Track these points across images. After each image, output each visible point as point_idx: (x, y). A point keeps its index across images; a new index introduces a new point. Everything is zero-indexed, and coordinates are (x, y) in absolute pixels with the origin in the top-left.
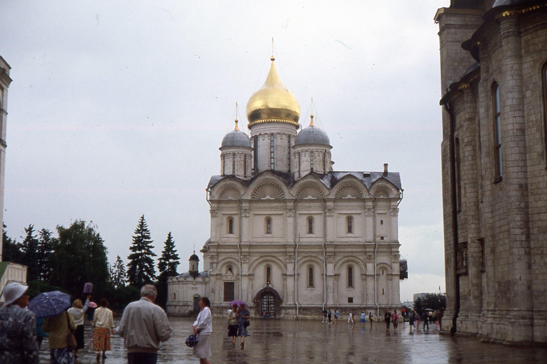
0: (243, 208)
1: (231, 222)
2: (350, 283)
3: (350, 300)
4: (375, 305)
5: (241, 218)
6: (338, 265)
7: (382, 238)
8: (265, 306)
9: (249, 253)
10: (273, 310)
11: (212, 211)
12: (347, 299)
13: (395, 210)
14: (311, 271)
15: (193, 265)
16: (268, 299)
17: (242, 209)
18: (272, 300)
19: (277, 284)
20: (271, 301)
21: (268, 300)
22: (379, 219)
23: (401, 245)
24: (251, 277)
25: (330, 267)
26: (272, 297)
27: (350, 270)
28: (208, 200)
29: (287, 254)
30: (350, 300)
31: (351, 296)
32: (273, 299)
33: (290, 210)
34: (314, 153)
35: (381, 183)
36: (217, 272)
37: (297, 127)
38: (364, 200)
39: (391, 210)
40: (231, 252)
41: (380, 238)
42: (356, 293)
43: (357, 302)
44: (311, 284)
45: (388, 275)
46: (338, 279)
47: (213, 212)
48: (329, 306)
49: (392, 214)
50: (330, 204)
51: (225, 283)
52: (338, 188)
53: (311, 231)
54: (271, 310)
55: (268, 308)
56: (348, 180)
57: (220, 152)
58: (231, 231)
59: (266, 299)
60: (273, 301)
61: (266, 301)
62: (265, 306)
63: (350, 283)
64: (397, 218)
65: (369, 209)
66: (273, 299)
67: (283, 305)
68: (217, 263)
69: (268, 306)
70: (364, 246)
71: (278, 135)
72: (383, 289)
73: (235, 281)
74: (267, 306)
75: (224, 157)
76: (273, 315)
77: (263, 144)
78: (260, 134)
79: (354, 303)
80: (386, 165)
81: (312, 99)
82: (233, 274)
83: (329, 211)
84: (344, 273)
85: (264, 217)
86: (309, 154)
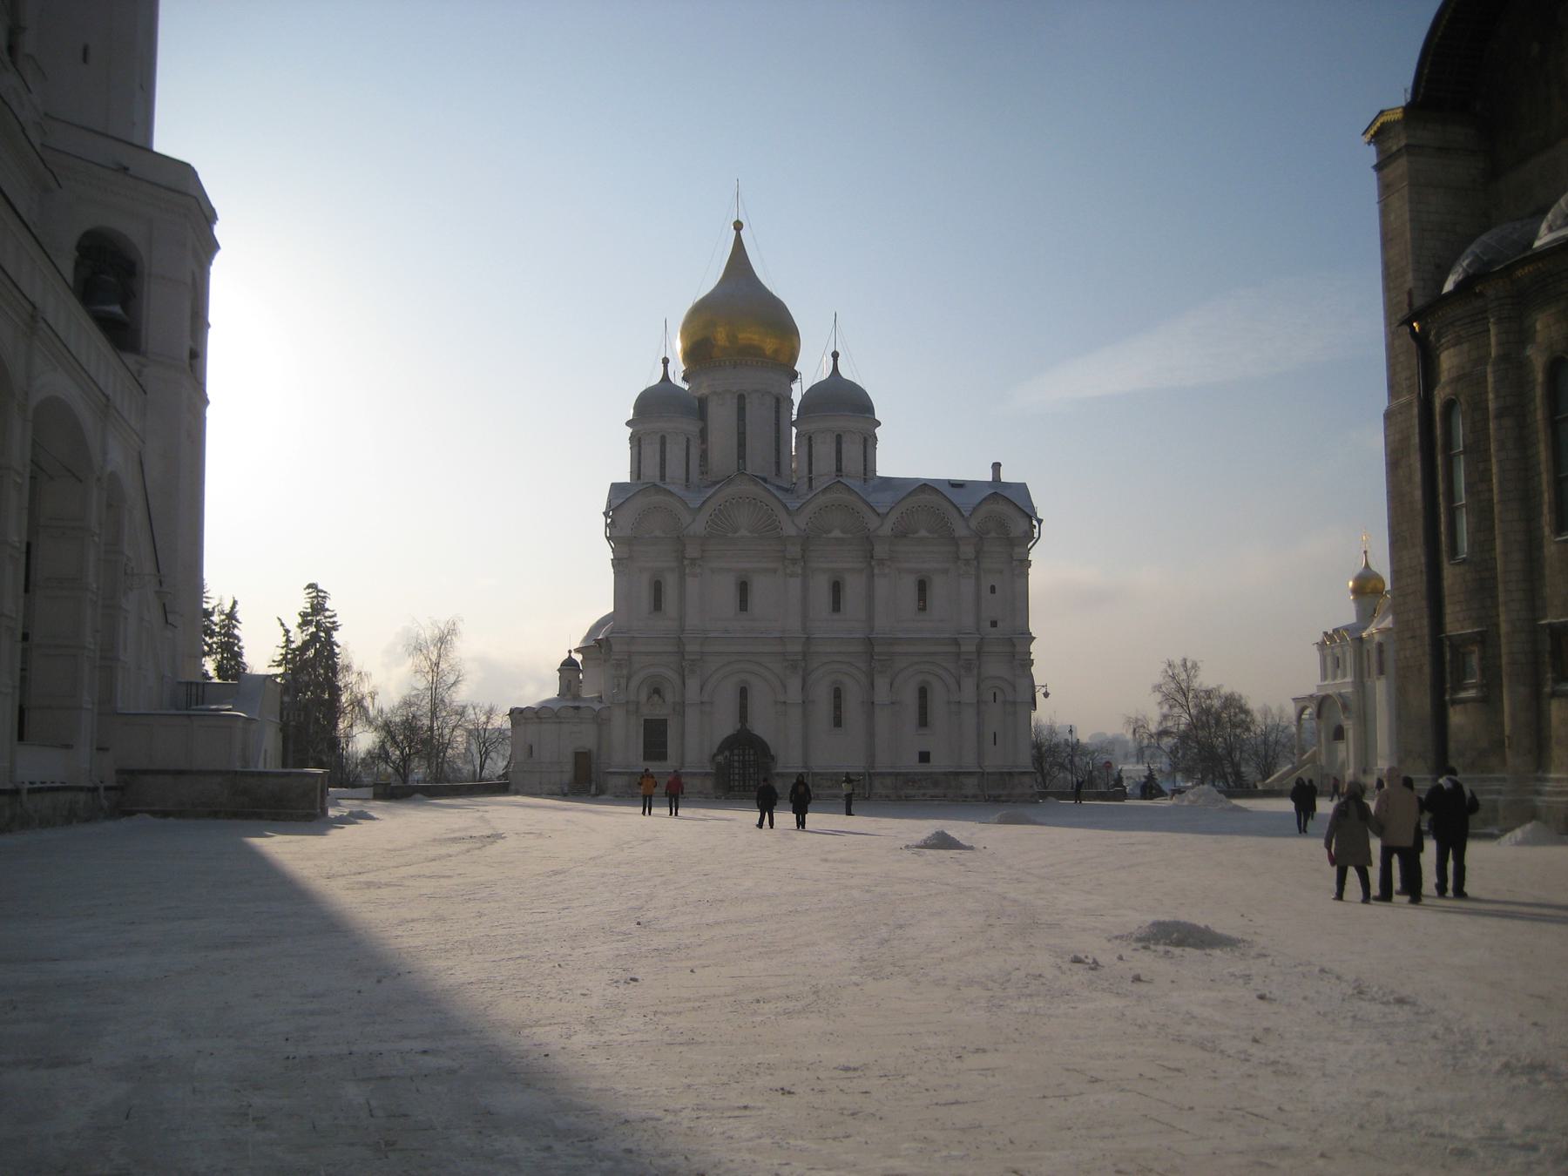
0: (687, 556)
1: (658, 588)
2: (923, 721)
3: (924, 757)
5: (682, 577)
7: (994, 624)
8: (737, 771)
11: (616, 562)
12: (917, 758)
14: (838, 694)
17: (684, 558)
19: (761, 726)
21: (744, 757)
23: (1035, 638)
25: (881, 683)
26: (752, 752)
27: (923, 693)
30: (924, 757)
31: (924, 749)
33: (794, 561)
37: (794, 376)
38: (954, 541)
39: (1014, 563)
41: (989, 623)
43: (939, 763)
44: (838, 722)
47: (617, 563)
51: (646, 721)
57: (629, 430)
58: (657, 604)
59: (739, 756)
62: (737, 771)
63: (923, 721)
67: (779, 770)
68: (629, 678)
70: (956, 642)
75: (639, 440)
77: (721, 417)
80: (996, 467)
82: (664, 701)
84: (910, 698)
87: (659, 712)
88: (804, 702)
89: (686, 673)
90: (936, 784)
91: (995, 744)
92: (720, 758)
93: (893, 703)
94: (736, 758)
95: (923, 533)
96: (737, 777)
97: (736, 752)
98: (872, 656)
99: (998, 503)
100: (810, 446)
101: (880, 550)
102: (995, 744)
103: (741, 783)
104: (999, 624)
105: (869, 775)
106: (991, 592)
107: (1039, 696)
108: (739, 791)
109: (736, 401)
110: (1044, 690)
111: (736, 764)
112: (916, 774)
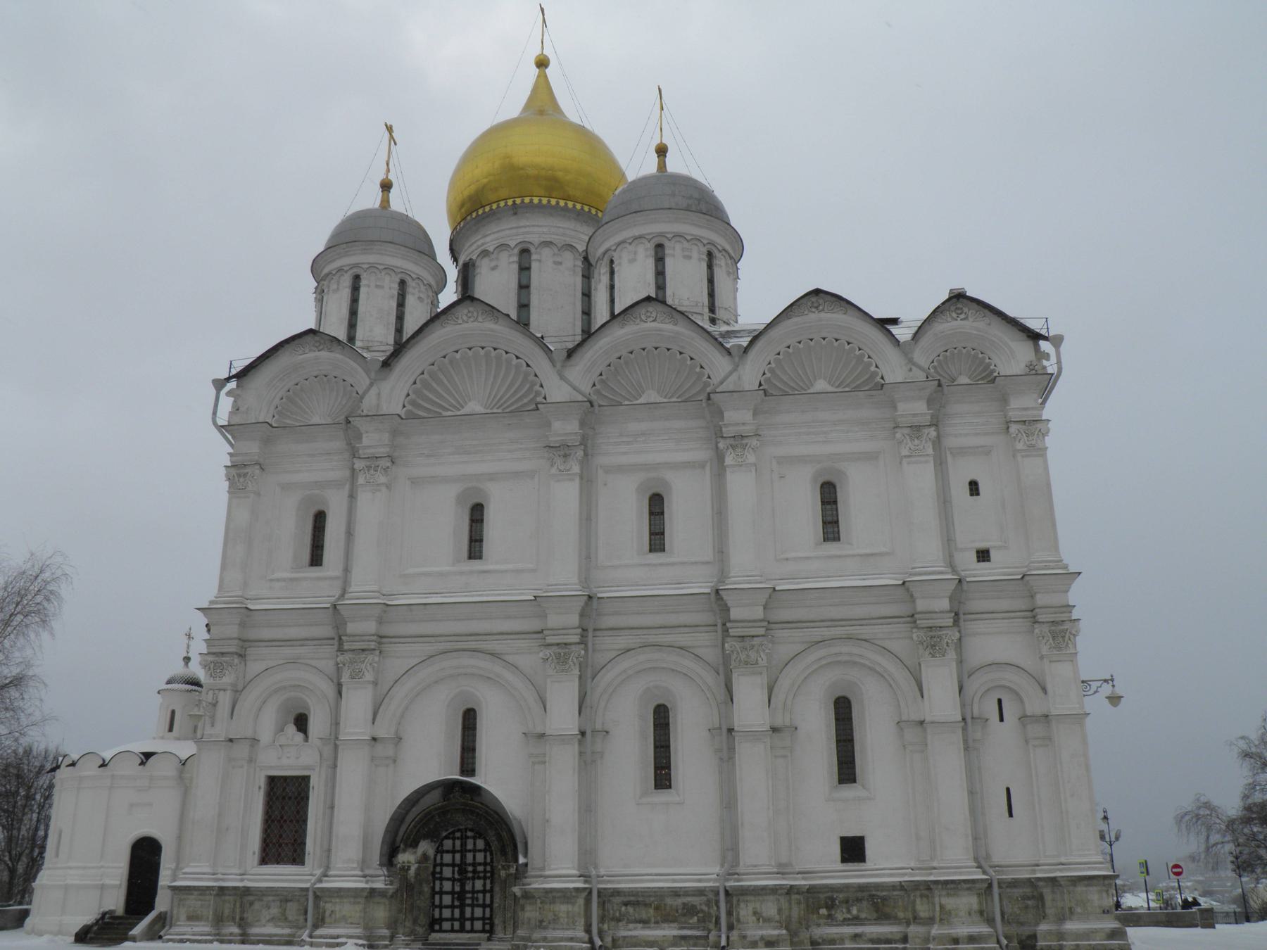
2: (847, 771)
3: (853, 849)
5: (352, 497)
6: (784, 684)
8: (447, 886)
9: (380, 643)
10: (484, 906)
11: (233, 471)
13: (1034, 426)
14: (662, 719)
15: (173, 712)
16: (463, 851)
18: (480, 857)
20: (474, 864)
21: (463, 857)
22: (961, 473)
25: (749, 691)
26: (480, 844)
27: (843, 711)
28: (220, 428)
29: (550, 640)
32: (485, 851)
34: (667, 244)
35: (959, 322)
39: (1014, 428)
40: (303, 641)
44: (663, 777)
45: (1024, 718)
47: (238, 472)
49: (1020, 446)
51: (272, 780)
52: (772, 357)
53: (657, 540)
54: (473, 906)
55: (461, 896)
56: (813, 317)
59: (453, 852)
60: (485, 864)
61: (453, 865)
62: (447, 886)
63: (847, 771)
64: (1046, 461)
66: (485, 851)
68: (237, 692)
69: (463, 886)
71: (546, 252)
72: (1008, 790)
74: (457, 889)
76: (483, 931)
78: (485, 253)
79: (869, 864)
81: (661, 129)
83: (733, 447)
86: (646, 250)
88: (583, 734)
89: (345, 679)
90: (882, 915)
91: (1011, 815)
93: (774, 730)
94: (447, 858)
96: (447, 900)
98: (726, 631)
99: (966, 319)
100: (612, 273)
101: (738, 417)
102: (1011, 815)
103: (457, 913)
105: (727, 893)
106: (972, 495)
107: (1096, 704)
108: (452, 931)
109: (515, 259)
110: (1107, 690)
111: (447, 872)
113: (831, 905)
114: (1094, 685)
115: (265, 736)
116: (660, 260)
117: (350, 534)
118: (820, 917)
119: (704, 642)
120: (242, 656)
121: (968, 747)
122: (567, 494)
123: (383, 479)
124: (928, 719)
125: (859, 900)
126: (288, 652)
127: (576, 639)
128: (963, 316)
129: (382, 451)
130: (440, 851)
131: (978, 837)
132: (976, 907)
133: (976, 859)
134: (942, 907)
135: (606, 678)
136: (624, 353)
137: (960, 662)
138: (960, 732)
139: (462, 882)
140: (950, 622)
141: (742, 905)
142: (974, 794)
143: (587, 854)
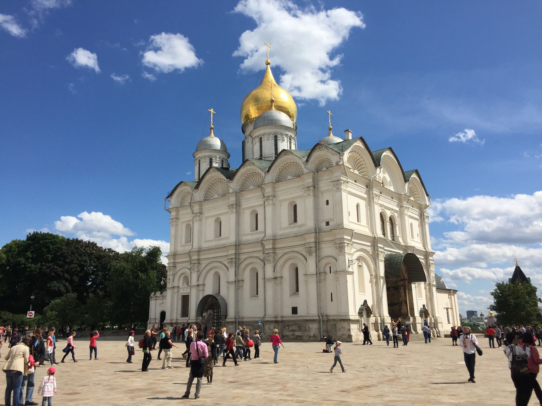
3: (295, 310)
4: (319, 316)
5: (193, 224)
7: (328, 224)
12: (290, 311)
21: (218, 314)
24: (201, 288)
35: (320, 152)
36: (176, 285)
41: (324, 224)
42: (299, 302)
46: (281, 283)
48: (267, 319)
50: (268, 191)
54: (220, 326)
55: (217, 323)
61: (216, 316)
65: (309, 187)
72: (331, 293)
73: (188, 293)
84: (287, 274)
85: (214, 218)
87: (184, 291)
91: (332, 301)
92: (205, 314)
95: (289, 177)
97: (215, 310)
98: (264, 251)
102: (332, 301)
104: (330, 223)
112: (289, 321)
113: (289, 326)
114: (354, 261)
115: (181, 286)
116: (261, 142)
117: (193, 233)
118: (286, 329)
119: (260, 255)
120: (175, 267)
121: (319, 282)
122: (233, 217)
123: (198, 219)
124: (308, 273)
125: (295, 325)
126: (183, 265)
127: (234, 257)
128: (321, 150)
129: (198, 211)
130: (214, 312)
131: (319, 308)
132: (317, 327)
133: (318, 315)
134: (309, 327)
135: (242, 266)
136: (246, 175)
137: (316, 256)
138: (315, 277)
139: (218, 320)
140: (314, 245)
141: (266, 326)
142: (319, 295)
143: (237, 312)
